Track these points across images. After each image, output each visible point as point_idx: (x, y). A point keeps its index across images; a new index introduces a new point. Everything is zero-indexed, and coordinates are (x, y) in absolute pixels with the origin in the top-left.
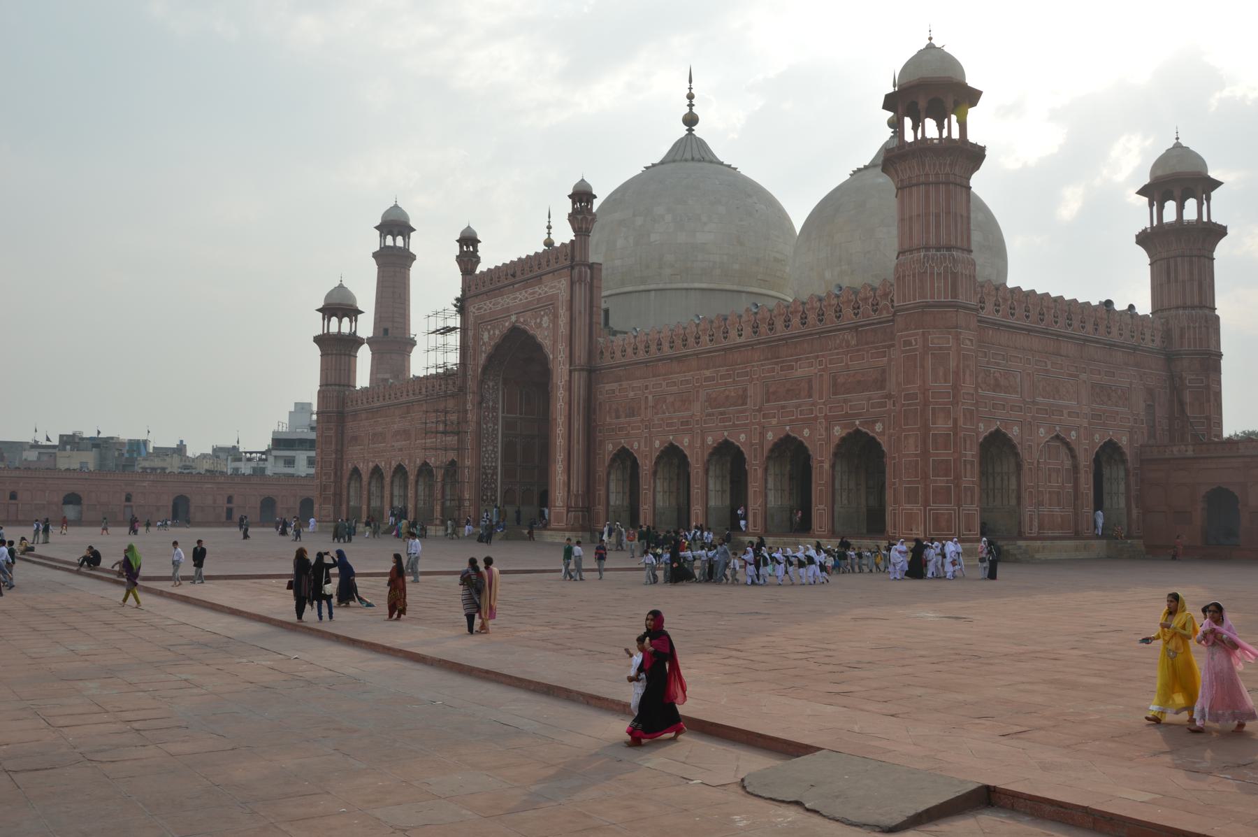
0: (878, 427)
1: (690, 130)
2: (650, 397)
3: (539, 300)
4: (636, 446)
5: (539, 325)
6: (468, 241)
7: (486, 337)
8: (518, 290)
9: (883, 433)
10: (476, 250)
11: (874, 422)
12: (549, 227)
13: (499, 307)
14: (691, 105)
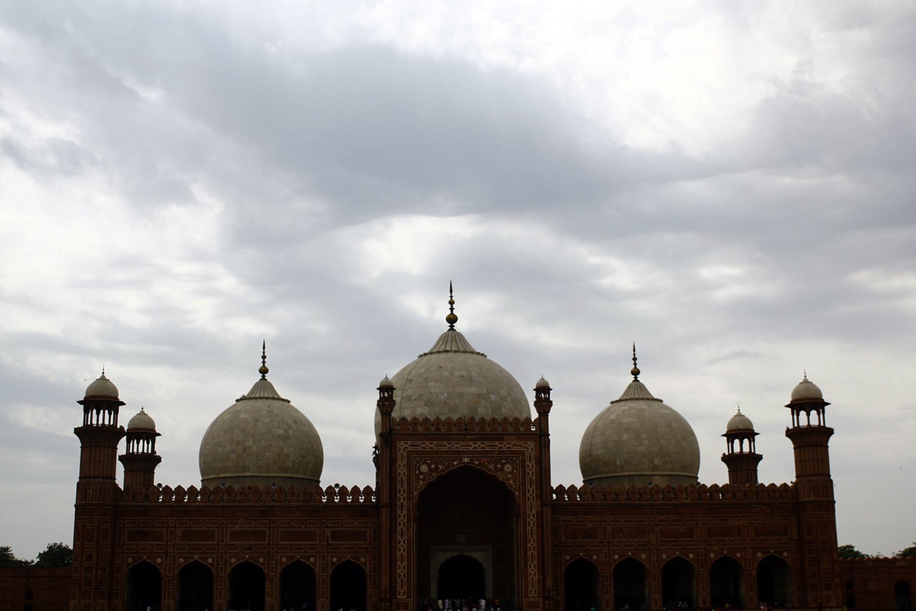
0: (785, 554)
1: (452, 327)
2: (608, 528)
3: (500, 452)
4: (595, 557)
5: (502, 469)
6: (386, 389)
7: (424, 468)
8: (471, 440)
9: (787, 557)
10: (391, 396)
11: (783, 552)
12: (264, 357)
13: (445, 449)
14: (452, 309)
